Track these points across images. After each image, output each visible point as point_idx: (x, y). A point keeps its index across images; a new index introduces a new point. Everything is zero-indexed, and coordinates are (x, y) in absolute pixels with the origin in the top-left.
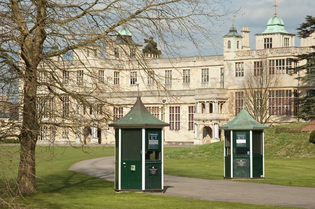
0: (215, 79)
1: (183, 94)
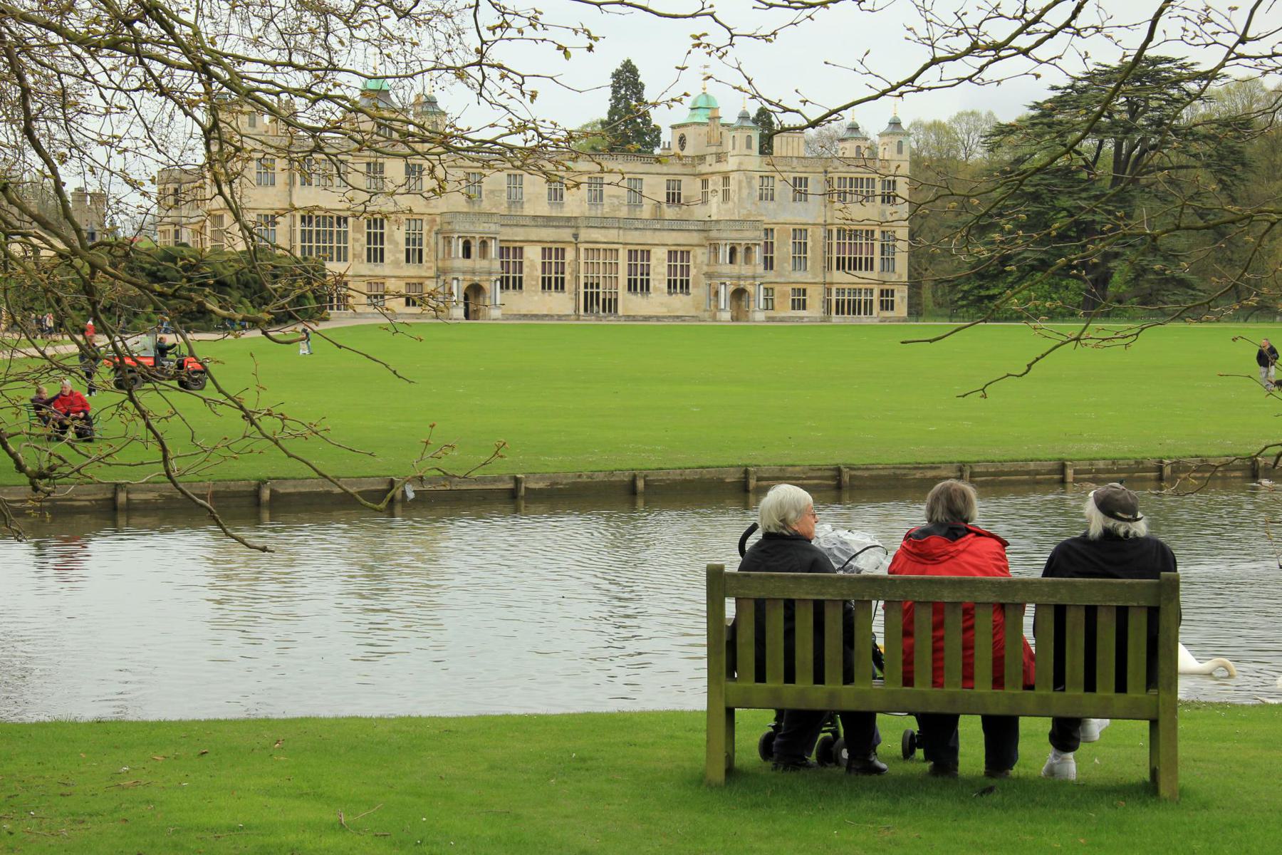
0: (618, 197)
1: (658, 226)
